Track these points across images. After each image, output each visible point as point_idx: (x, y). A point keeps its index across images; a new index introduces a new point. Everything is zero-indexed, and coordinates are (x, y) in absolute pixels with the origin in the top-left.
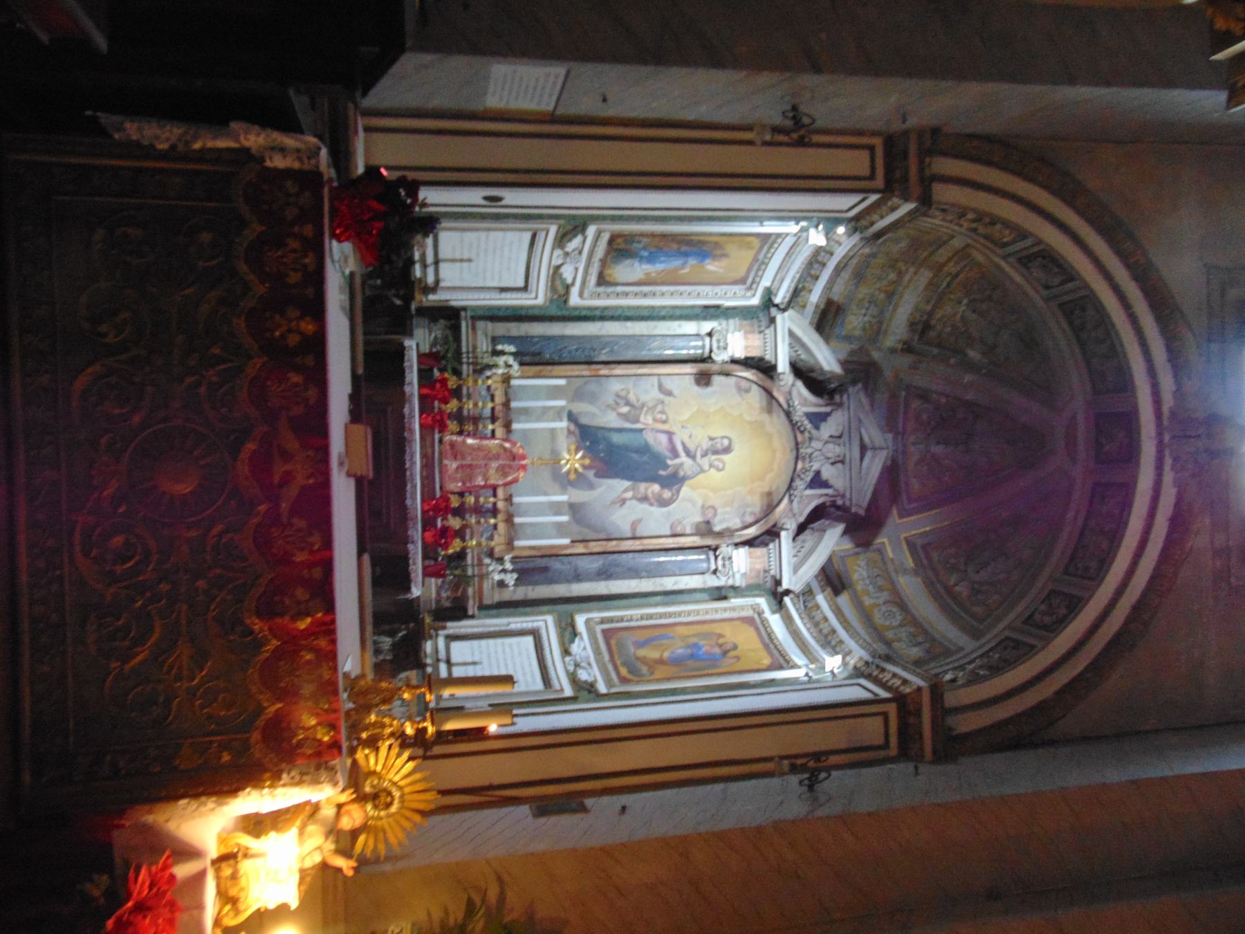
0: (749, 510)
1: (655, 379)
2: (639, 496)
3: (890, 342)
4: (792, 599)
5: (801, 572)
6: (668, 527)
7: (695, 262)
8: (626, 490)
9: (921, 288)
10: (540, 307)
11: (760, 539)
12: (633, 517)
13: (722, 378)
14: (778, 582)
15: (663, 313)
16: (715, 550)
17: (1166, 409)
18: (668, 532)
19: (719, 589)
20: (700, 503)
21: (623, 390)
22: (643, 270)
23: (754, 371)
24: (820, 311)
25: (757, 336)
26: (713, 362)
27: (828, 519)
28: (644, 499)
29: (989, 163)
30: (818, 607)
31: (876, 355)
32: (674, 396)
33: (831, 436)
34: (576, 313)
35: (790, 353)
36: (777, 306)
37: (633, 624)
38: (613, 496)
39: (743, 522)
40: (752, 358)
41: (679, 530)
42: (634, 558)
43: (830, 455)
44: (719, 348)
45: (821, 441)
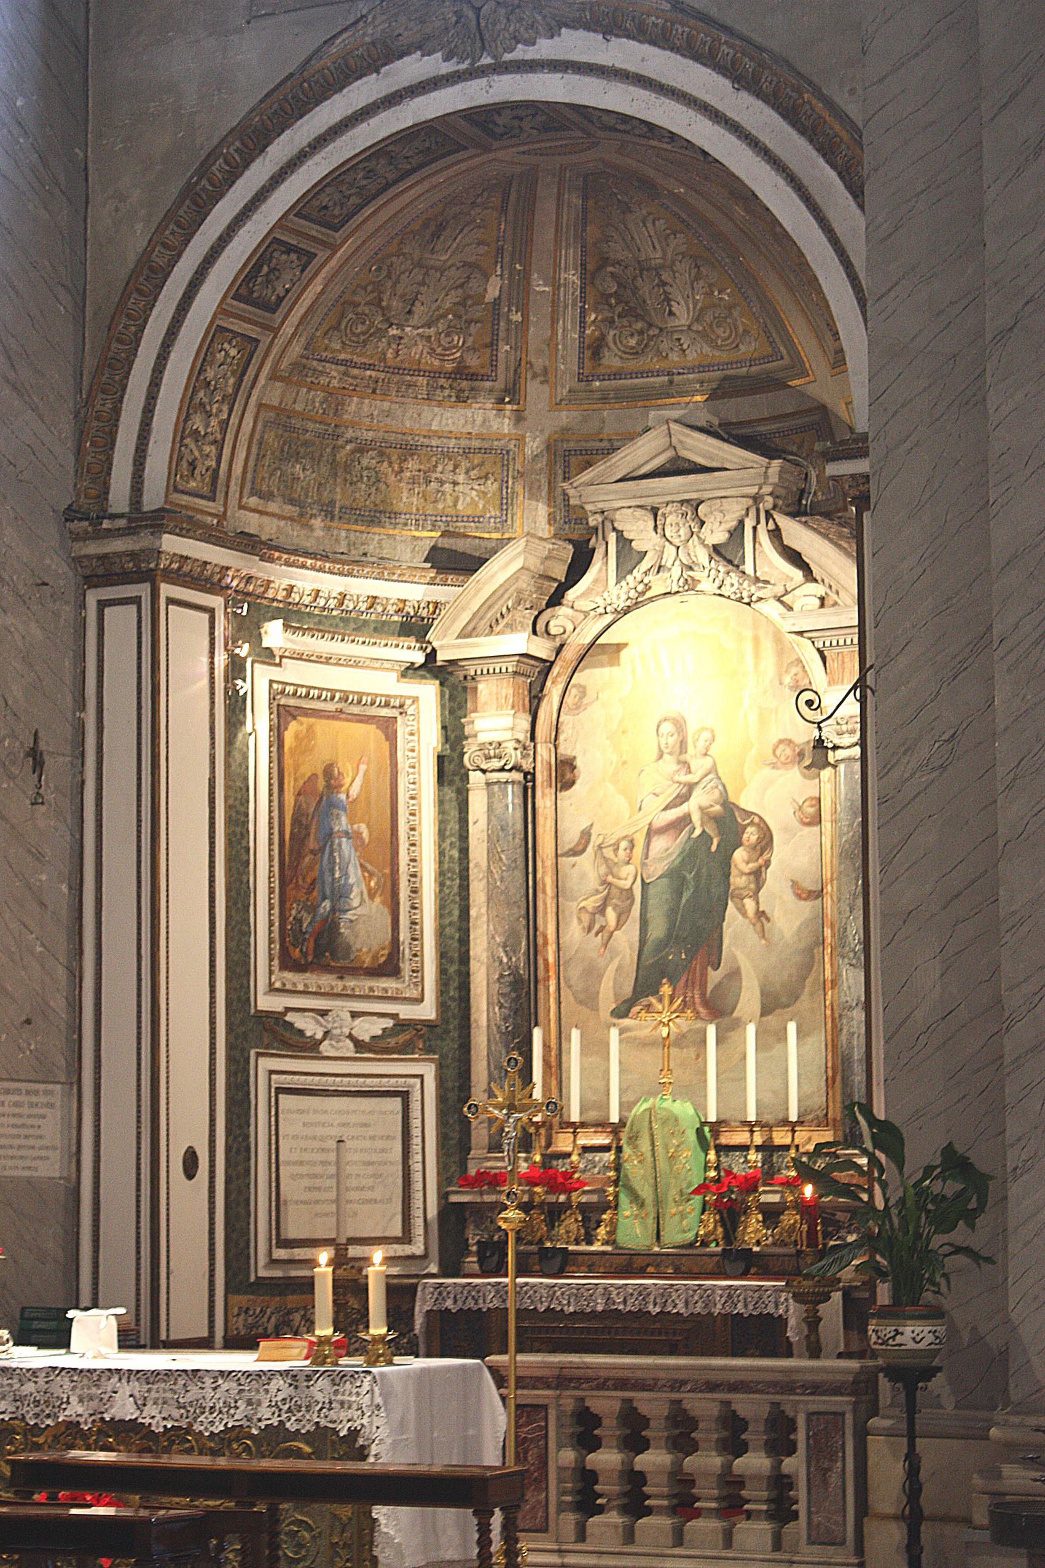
2: (752, 886)
3: (504, 425)
7: (344, 819)
8: (744, 914)
9: (386, 405)
10: (440, 1067)
12: (789, 896)
15: (455, 853)
17: (447, 68)
20: (767, 771)
21: (579, 919)
22: (362, 902)
28: (758, 876)
29: (117, 411)
31: (533, 445)
38: (751, 936)
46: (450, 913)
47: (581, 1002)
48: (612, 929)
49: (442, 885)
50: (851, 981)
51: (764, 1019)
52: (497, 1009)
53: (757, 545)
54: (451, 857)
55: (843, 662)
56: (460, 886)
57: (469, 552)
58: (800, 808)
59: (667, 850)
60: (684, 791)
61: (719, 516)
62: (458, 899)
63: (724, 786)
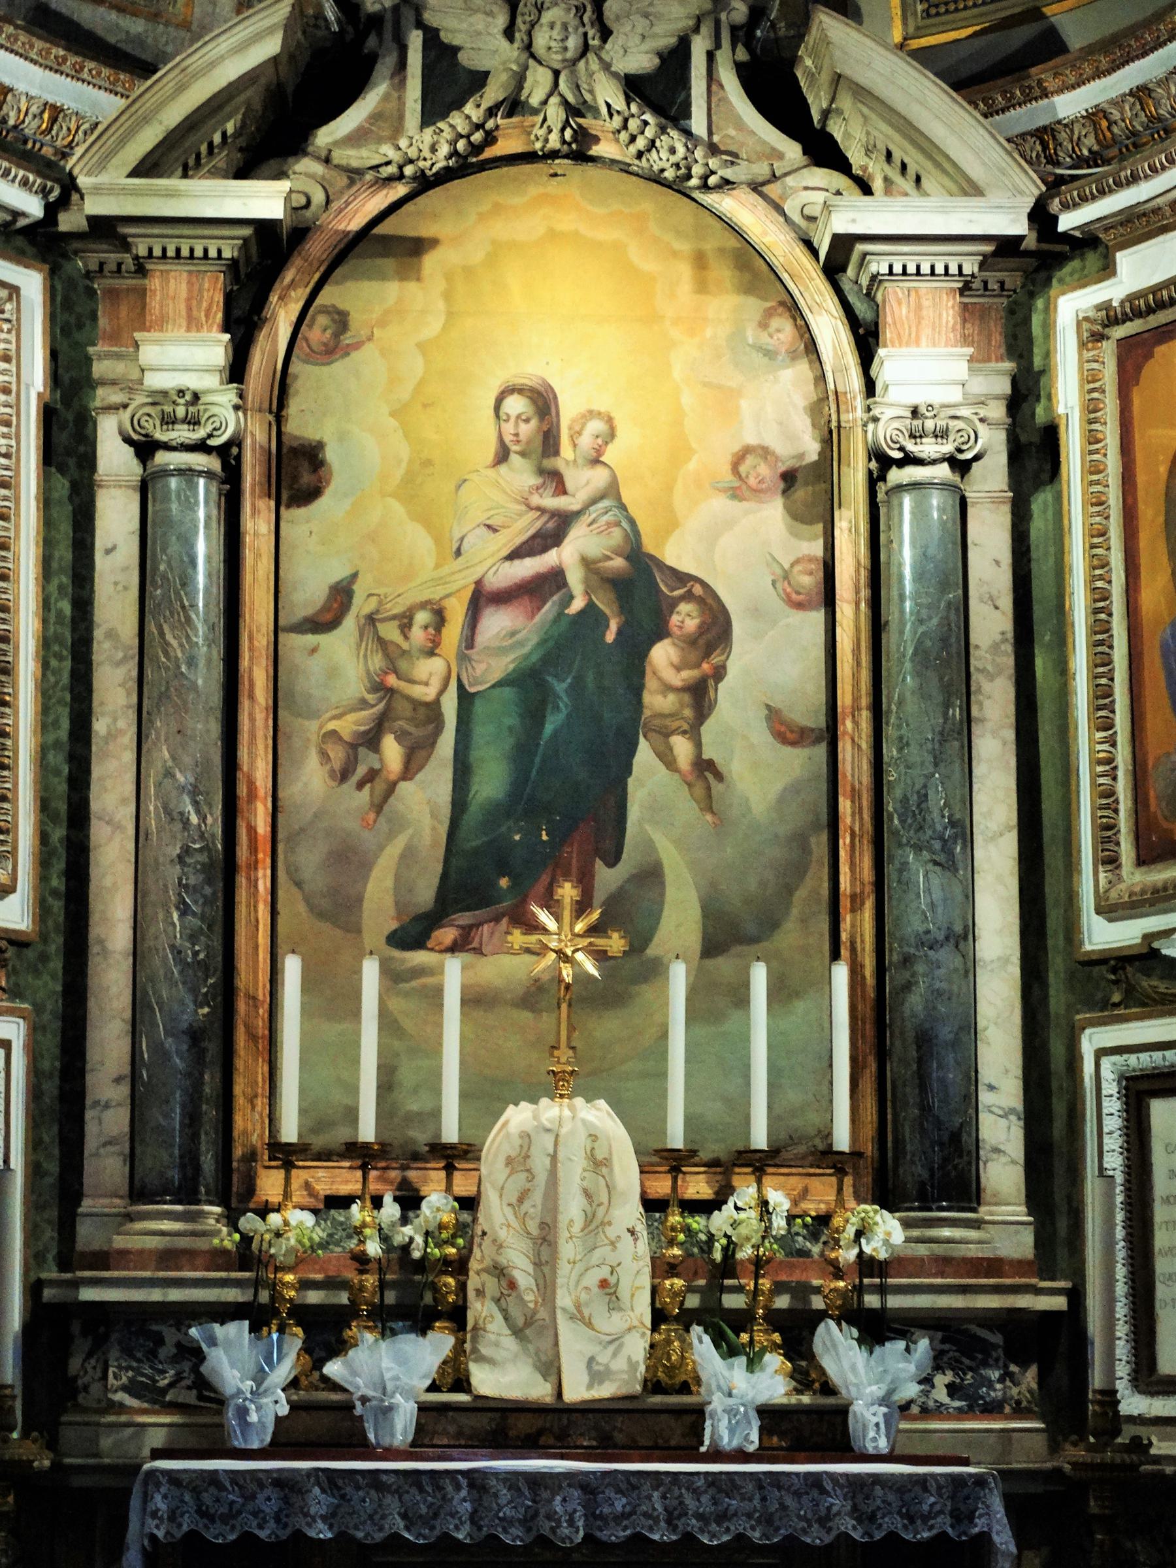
0: (751, 334)
1: (294, 643)
2: (688, 713)
4: (1066, 207)
5: (975, 170)
6: (797, 617)
10: (35, 1030)
11: (851, 299)
12: (761, 735)
13: (294, 407)
14: (1006, 246)
15: (66, 607)
16: (883, 462)
18: (818, 617)
19: (1016, 453)
20: (720, 504)
21: (324, 756)
23: (274, 298)
24: (73, 59)
25: (154, 283)
26: (236, 442)
27: (793, 60)
30: (1095, 116)
32: (354, 576)
33: (509, 33)
34: (57, 905)
35: (215, 173)
36: (52, 210)
37: (1123, 755)
38: (685, 807)
39: (793, 356)
40: (229, 300)
41: (809, 581)
42: (903, 744)
43: (573, 43)
44: (194, 422)
45: (526, 68)
46: (56, 724)
47: (321, 915)
48: (393, 777)
49: (45, 665)
50: (937, 895)
51: (710, 963)
52: (175, 916)
53: (714, 88)
54: (60, 613)
55: (919, 307)
56: (74, 674)
57: (100, 32)
58: (786, 576)
59: (513, 634)
60: (551, 525)
61: (641, 24)
62: (68, 697)
63: (632, 522)
